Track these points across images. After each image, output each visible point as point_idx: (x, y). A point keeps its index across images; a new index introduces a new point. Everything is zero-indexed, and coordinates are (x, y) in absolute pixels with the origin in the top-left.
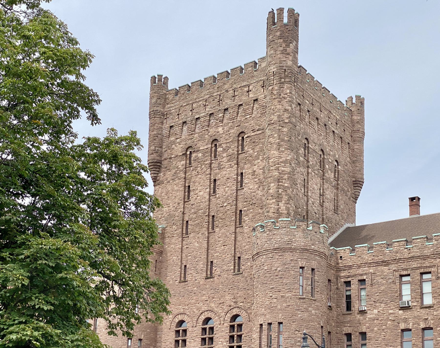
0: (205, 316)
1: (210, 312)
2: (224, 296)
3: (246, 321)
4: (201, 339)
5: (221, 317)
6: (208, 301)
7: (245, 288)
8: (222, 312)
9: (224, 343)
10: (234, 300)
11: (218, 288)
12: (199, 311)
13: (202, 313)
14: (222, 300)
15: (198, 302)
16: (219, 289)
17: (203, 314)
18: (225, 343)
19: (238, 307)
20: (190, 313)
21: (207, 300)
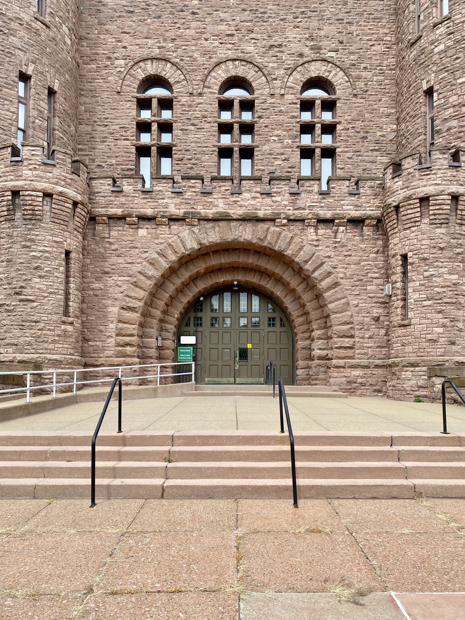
0: (226, 71)
1: (244, 63)
2: (283, 31)
3: (347, 94)
4: (216, 125)
5: (275, 79)
6: (235, 38)
7: (341, 17)
8: (278, 68)
9: (285, 141)
10: (308, 43)
11: (262, 10)
12: (210, 58)
13: (218, 64)
14: (277, 40)
15: (204, 36)
16: (265, 13)
17: (223, 66)
18: (290, 141)
19: (324, 60)
20: (182, 60)
21: (232, 35)
